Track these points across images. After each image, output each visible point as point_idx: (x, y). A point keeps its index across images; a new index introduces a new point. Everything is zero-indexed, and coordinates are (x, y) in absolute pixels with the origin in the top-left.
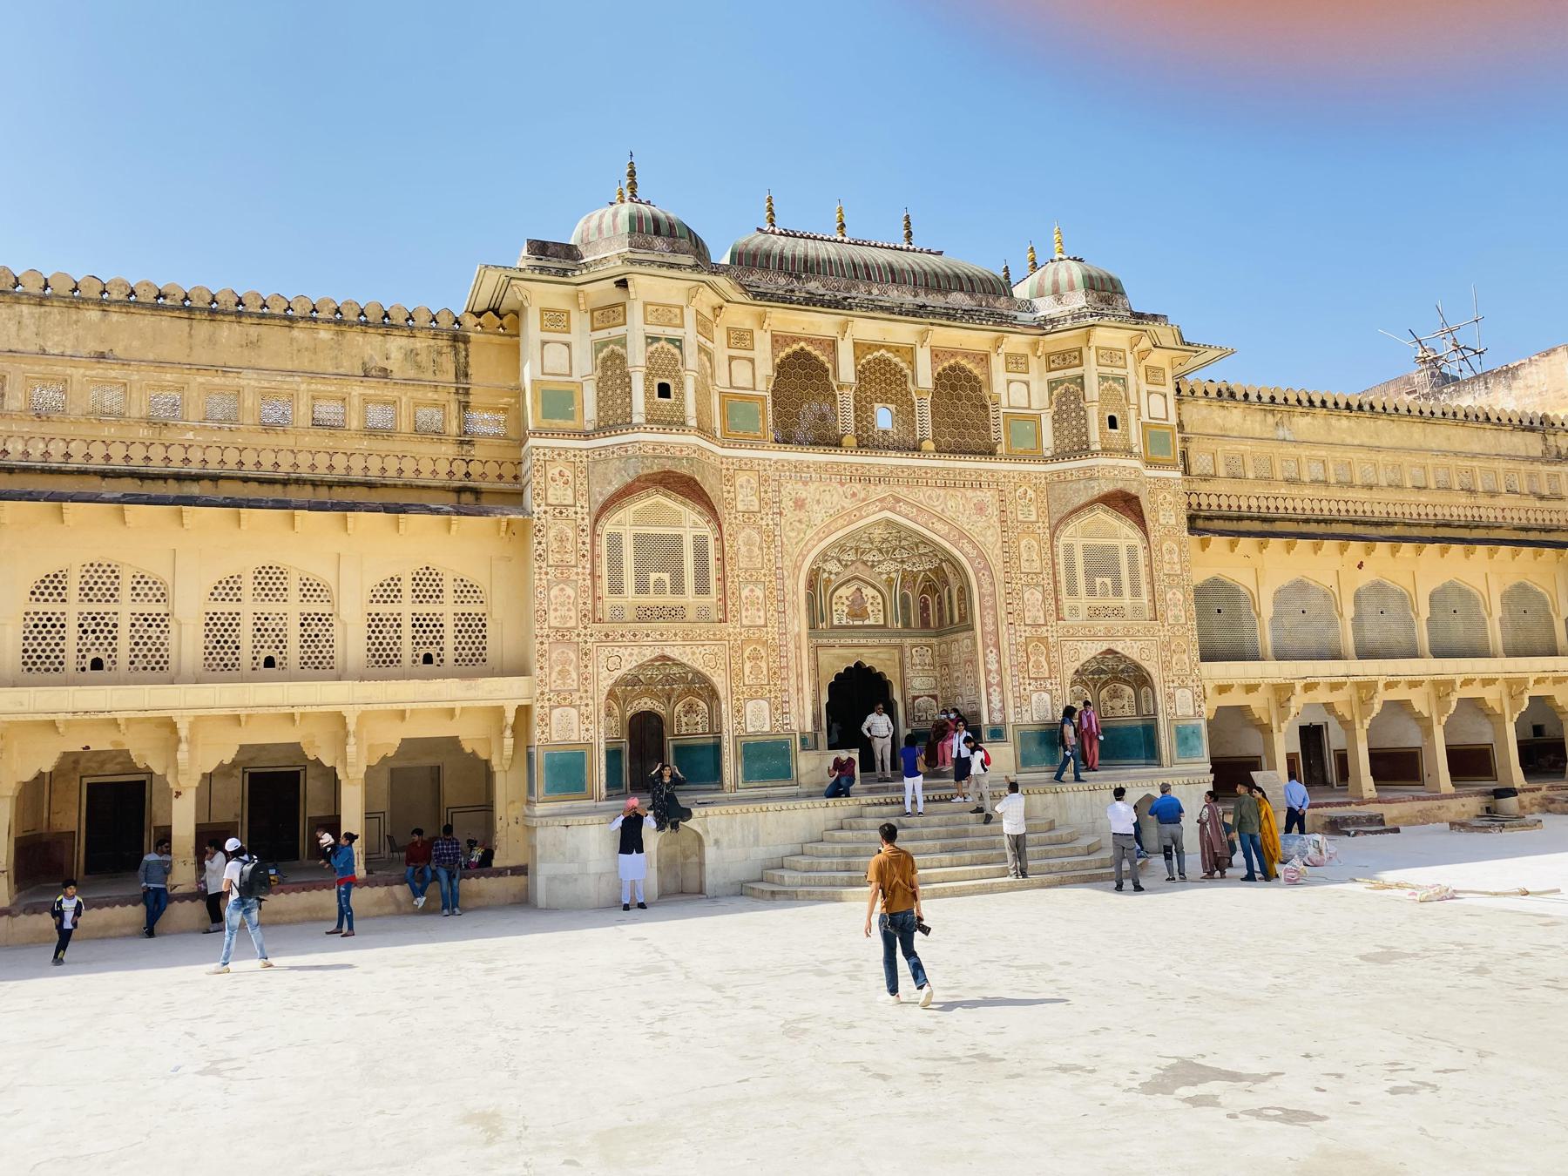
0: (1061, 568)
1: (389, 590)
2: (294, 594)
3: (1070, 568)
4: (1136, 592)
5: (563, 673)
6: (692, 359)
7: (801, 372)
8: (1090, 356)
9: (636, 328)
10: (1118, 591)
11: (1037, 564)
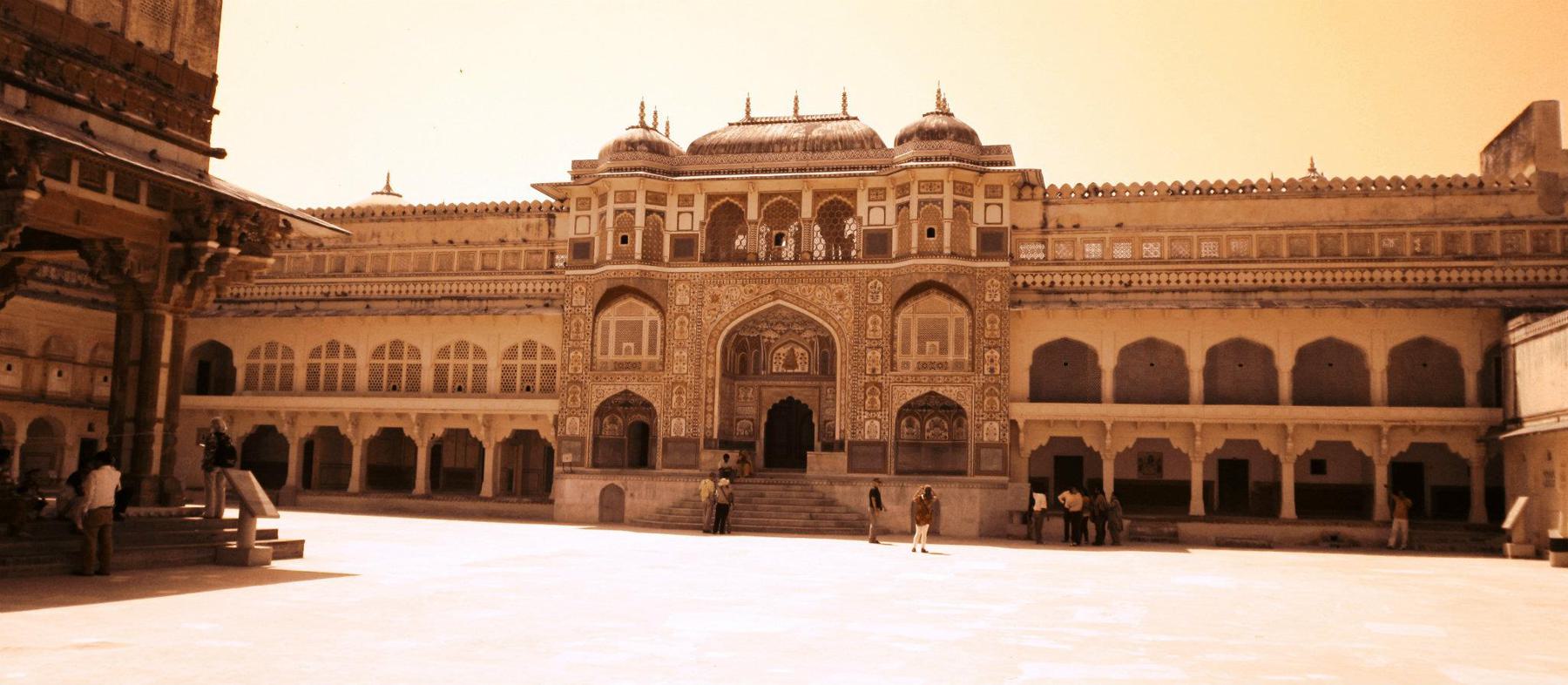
0: (899, 333)
1: (511, 353)
2: (471, 355)
3: (906, 337)
4: (959, 350)
5: (574, 400)
6: (640, 220)
7: (726, 215)
8: (914, 188)
9: (611, 207)
10: (944, 350)
11: (879, 334)
